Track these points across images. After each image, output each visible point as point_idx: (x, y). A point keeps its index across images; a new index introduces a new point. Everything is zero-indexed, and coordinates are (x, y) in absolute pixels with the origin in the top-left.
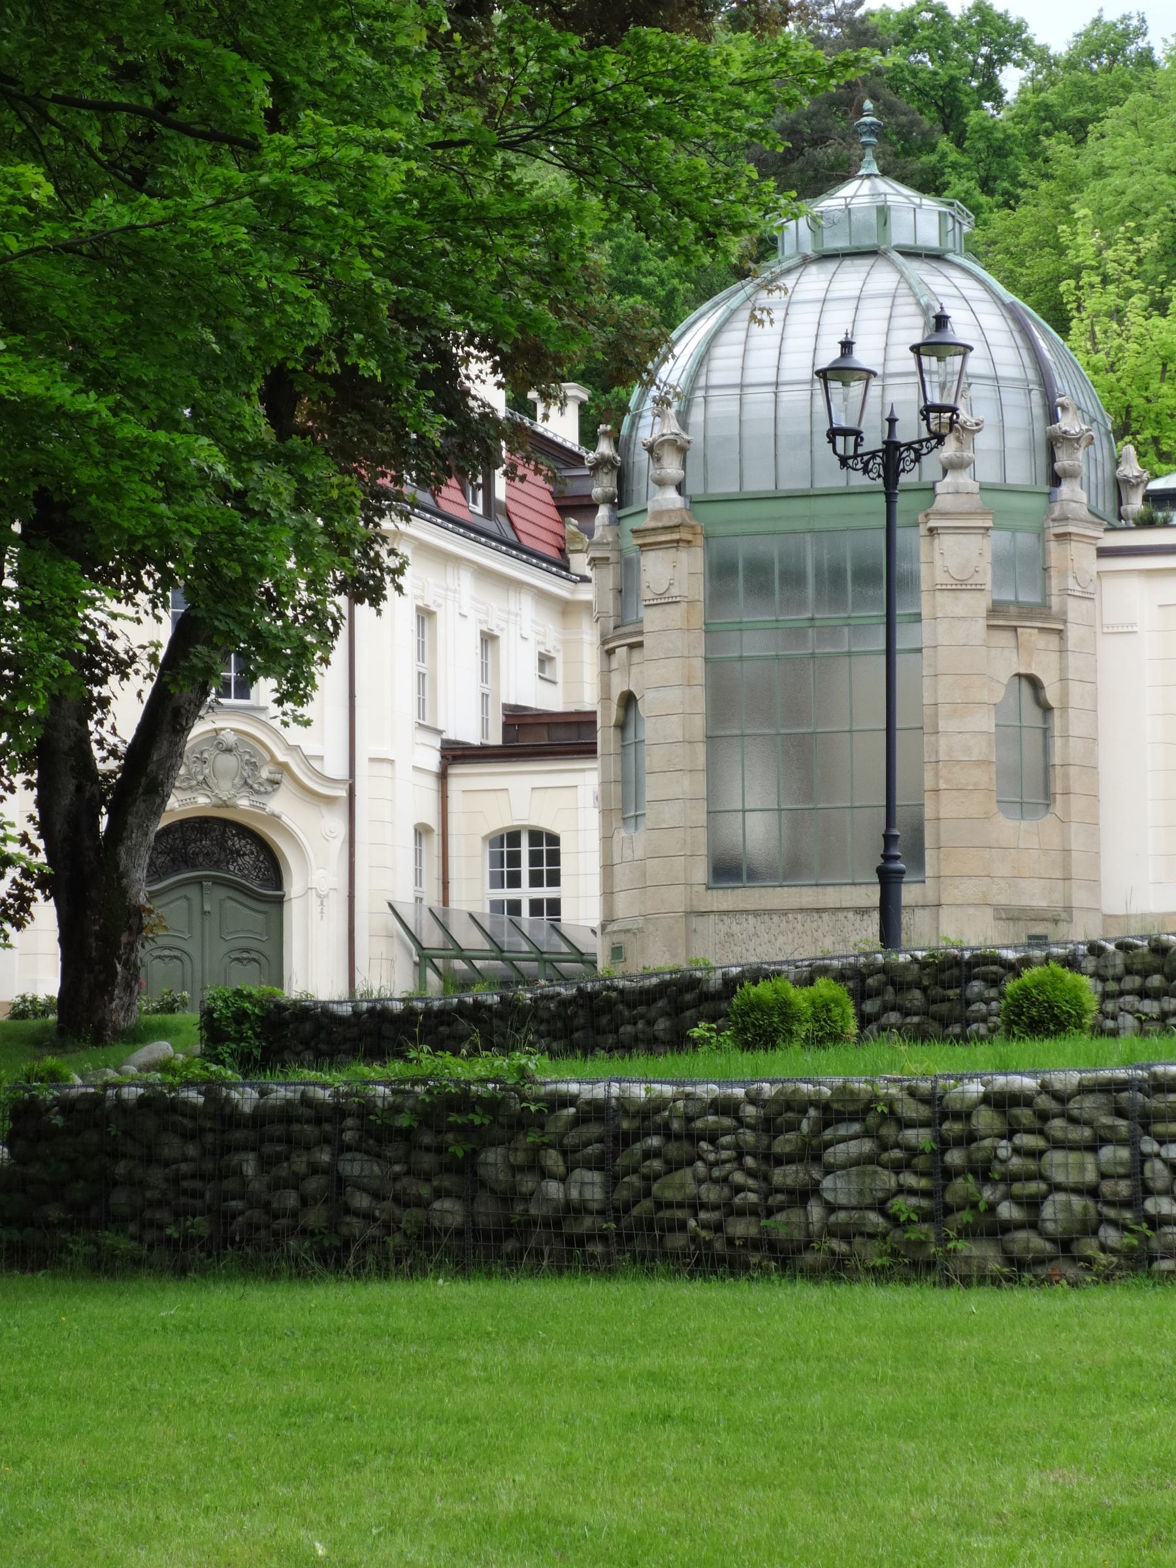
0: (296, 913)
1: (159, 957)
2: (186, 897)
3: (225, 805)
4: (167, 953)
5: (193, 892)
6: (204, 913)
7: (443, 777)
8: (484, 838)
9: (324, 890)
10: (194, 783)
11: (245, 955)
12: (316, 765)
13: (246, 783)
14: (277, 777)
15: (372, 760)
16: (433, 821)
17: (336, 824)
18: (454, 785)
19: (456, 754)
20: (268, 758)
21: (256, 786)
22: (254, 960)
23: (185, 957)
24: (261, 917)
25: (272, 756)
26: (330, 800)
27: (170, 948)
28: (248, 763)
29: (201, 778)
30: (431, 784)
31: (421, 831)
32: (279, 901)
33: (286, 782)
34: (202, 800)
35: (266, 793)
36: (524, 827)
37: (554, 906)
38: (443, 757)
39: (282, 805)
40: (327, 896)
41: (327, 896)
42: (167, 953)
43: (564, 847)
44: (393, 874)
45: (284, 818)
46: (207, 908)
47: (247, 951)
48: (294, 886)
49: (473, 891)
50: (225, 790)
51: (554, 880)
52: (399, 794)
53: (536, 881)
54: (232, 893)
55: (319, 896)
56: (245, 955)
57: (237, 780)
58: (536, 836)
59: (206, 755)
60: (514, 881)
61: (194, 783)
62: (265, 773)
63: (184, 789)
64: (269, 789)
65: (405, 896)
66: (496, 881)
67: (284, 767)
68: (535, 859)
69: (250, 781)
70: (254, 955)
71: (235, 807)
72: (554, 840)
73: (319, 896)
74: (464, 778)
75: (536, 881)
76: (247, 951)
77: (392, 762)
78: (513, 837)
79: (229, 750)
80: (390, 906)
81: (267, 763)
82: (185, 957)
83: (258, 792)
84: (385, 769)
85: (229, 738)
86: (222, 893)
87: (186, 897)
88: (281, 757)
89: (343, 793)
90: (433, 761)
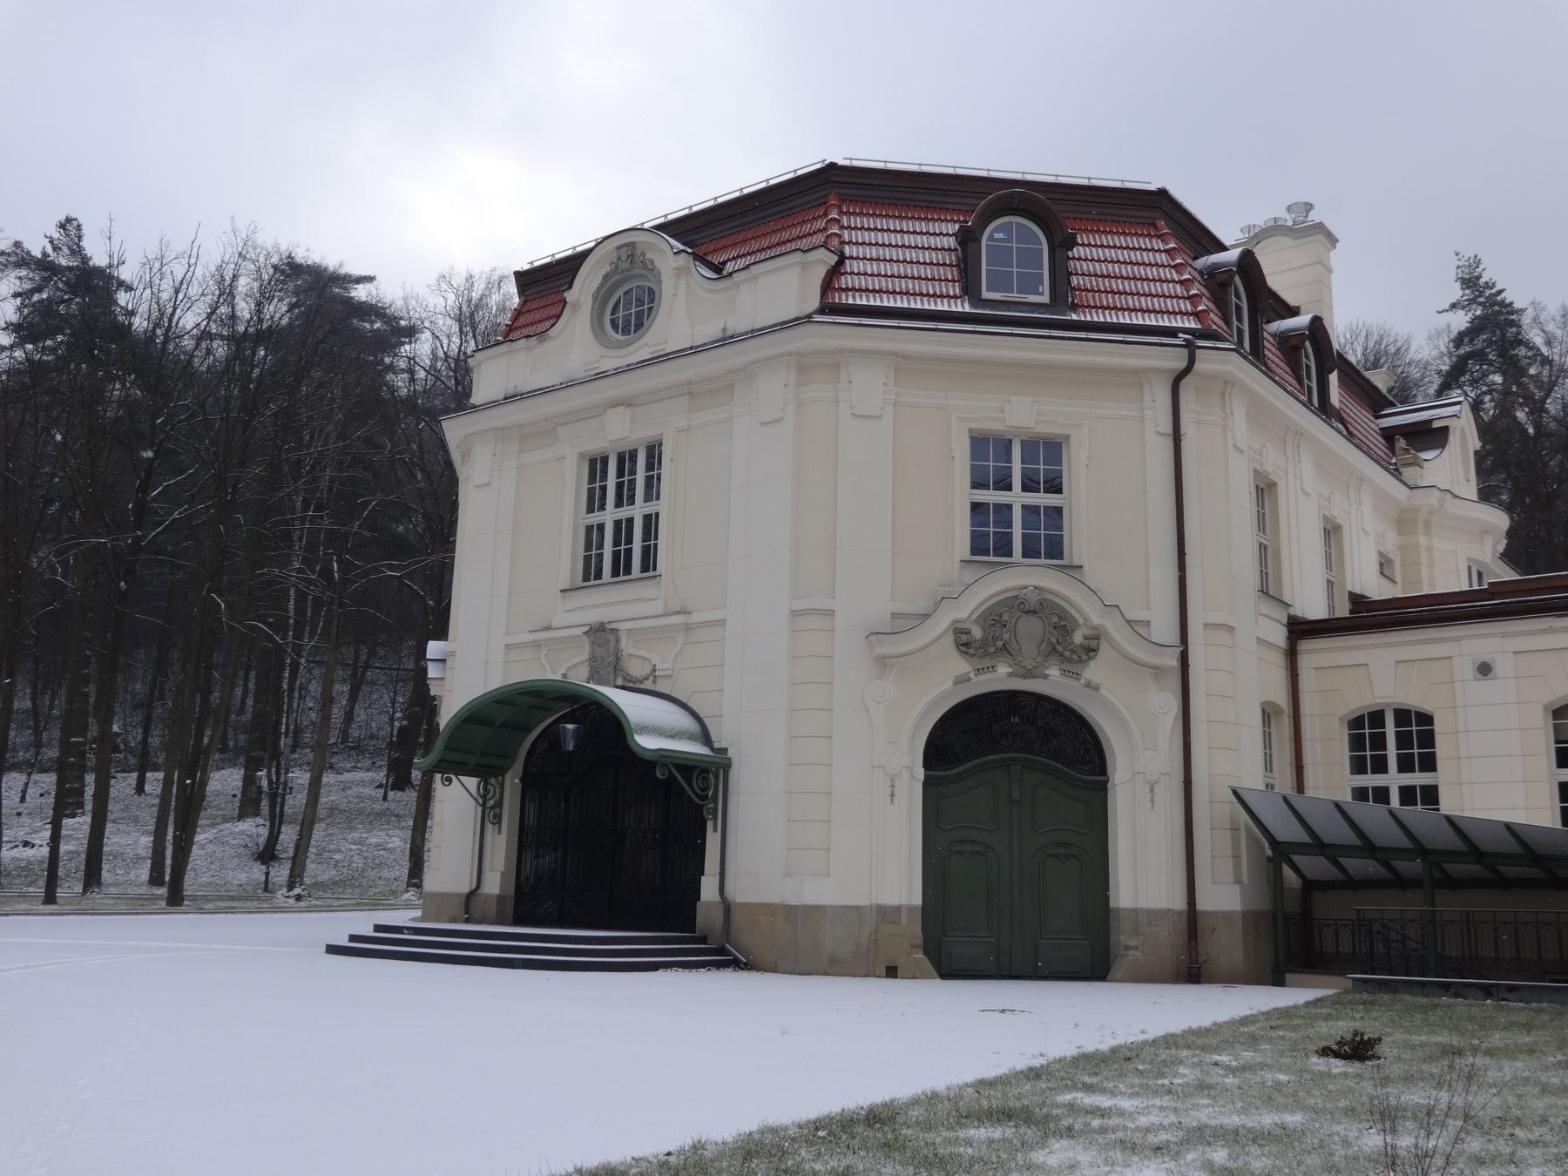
1: (957, 852)
4: (968, 847)
7: (1292, 654)
8: (1341, 719)
11: (1062, 851)
15: (1207, 626)
16: (1281, 698)
18: (1306, 662)
19: (1300, 630)
21: (1067, 654)
26: (1158, 671)
29: (1000, 644)
30: (1278, 662)
31: (1268, 714)
32: (1101, 788)
36: (1388, 705)
37: (1431, 795)
38: (1290, 632)
40: (1156, 782)
43: (1438, 727)
44: (1236, 759)
46: (1016, 795)
49: (1332, 777)
51: (1429, 764)
52: (1239, 672)
53: (1405, 765)
58: (1402, 716)
60: (1380, 766)
64: (1084, 657)
65: (1252, 778)
66: (1358, 767)
68: (1403, 740)
69: (1059, 648)
72: (1426, 719)
74: (1315, 654)
75: (1405, 765)
78: (1377, 717)
80: (1235, 793)
83: (1070, 660)
89: (1172, 661)
90: (1279, 635)
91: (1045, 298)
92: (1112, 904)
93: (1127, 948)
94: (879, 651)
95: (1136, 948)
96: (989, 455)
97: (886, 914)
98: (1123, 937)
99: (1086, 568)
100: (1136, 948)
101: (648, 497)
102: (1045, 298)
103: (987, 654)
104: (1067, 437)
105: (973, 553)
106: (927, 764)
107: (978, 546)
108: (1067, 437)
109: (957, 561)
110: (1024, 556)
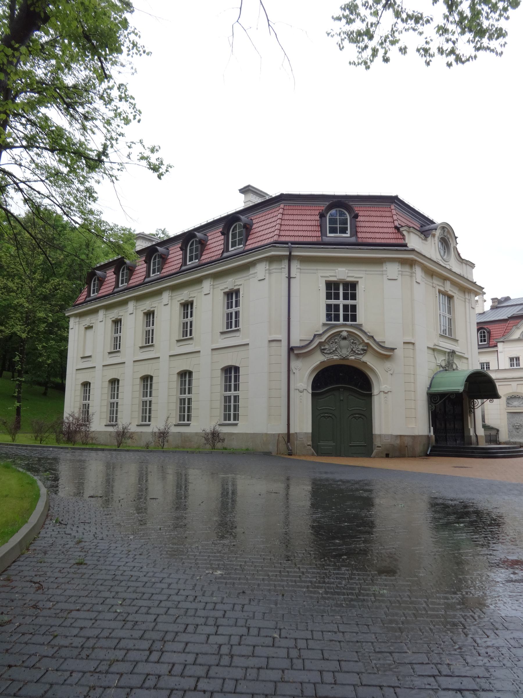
4: (326, 415)
14: (366, 348)
21: (357, 352)
22: (360, 417)
25: (363, 340)
27: (327, 413)
32: (370, 396)
34: (335, 357)
35: (361, 354)
39: (368, 359)
42: (326, 415)
45: (368, 363)
46: (342, 398)
62: (361, 347)
63: (329, 354)
64: (362, 352)
67: (367, 345)
71: (348, 359)
77: (413, 344)
79: (344, 338)
84: (411, 346)
85: (345, 334)
88: (366, 341)
91: (348, 235)
96: (332, 288)
98: (377, 442)
99: (363, 325)
101: (236, 306)
102: (348, 235)
103: (330, 353)
104: (358, 282)
105: (327, 321)
106: (313, 388)
107: (329, 317)
108: (358, 282)
109: (321, 324)
110: (344, 321)
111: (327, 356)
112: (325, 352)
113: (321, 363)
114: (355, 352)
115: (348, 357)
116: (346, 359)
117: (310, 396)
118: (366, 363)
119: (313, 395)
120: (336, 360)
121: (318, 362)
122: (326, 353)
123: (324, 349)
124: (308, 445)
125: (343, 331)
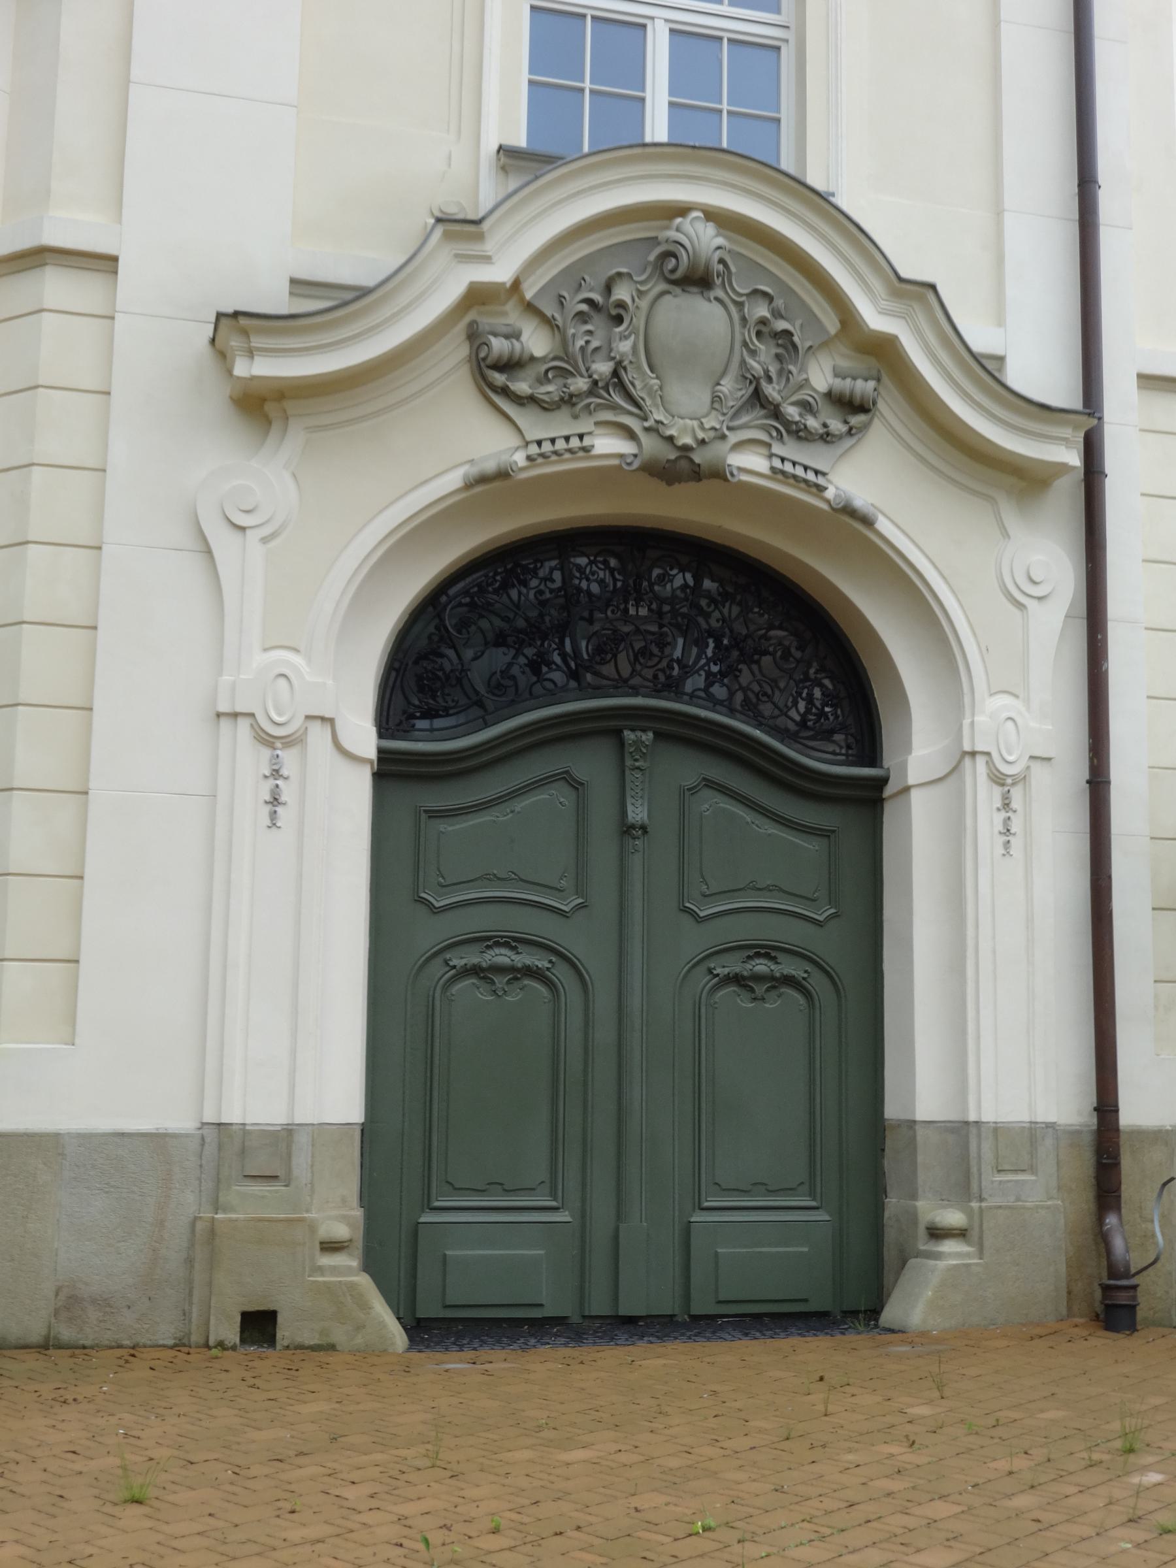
0: (919, 831)
1: (475, 971)
2: (577, 785)
3: (681, 469)
4: (502, 956)
5: (591, 763)
6: (627, 830)
9: (1013, 762)
10: (580, 384)
11: (761, 966)
12: (990, 365)
13: (758, 398)
14: (863, 388)
15: (1150, 382)
17: (1044, 556)
20: (831, 324)
21: (792, 412)
22: (789, 981)
23: (562, 974)
24: (811, 846)
28: (763, 329)
29: (603, 368)
32: (869, 802)
33: (890, 407)
35: (826, 437)
40: (1022, 779)
41: (1022, 779)
42: (502, 956)
47: (767, 952)
48: (918, 751)
50: (687, 410)
54: (720, 771)
55: (998, 779)
56: (761, 966)
57: (727, 385)
59: (622, 293)
61: (580, 384)
62: (820, 376)
64: (836, 426)
69: (771, 391)
70: (540, 961)
71: (719, 474)
73: (998, 779)
76: (767, 952)
79: (699, 280)
81: (827, 344)
82: (562, 974)
83: (799, 433)
86: (685, 768)
87: (577, 785)
89: (1074, 458)
92: (892, 1111)
93: (937, 1233)
94: (242, 368)
95: (961, 1234)
97: (248, 1155)
100: (961, 1234)
103: (568, 401)
106: (389, 720)
109: (490, 145)
111: (536, 426)
112: (522, 387)
113: (473, 483)
114: (776, 413)
115: (718, 450)
116: (697, 474)
117: (355, 793)
118: (868, 521)
119: (389, 772)
120: (609, 476)
121: (453, 480)
122: (530, 400)
123: (510, 365)
124: (331, 1247)
125: (682, 210)
